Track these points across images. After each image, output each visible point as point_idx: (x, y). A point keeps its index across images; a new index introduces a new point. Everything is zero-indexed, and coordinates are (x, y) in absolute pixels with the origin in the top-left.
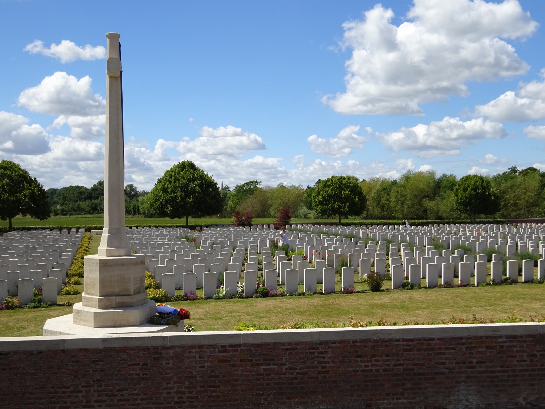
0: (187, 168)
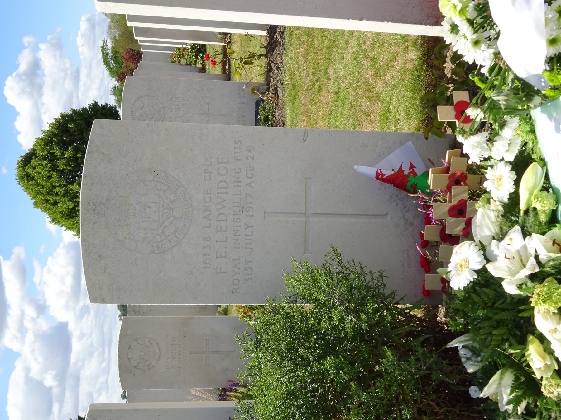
0: (29, 170)
